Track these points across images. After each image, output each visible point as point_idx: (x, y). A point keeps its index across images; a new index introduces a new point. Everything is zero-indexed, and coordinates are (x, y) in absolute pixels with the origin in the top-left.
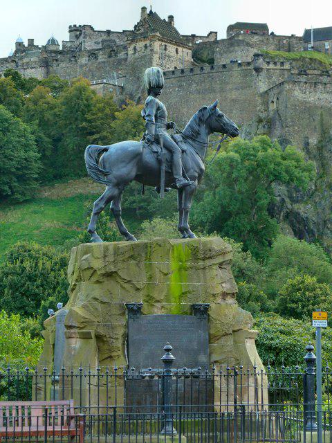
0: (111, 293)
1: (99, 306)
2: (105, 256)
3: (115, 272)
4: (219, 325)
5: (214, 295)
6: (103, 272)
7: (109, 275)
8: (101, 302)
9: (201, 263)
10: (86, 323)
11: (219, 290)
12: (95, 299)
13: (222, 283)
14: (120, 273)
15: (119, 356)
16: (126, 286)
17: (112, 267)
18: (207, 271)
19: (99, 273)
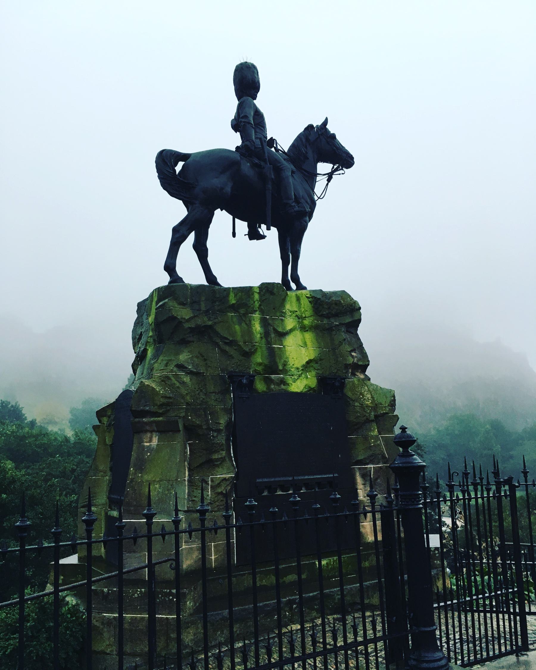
0: (205, 360)
1: (187, 379)
2: (193, 302)
3: (210, 327)
4: (358, 409)
5: (347, 366)
6: (192, 325)
7: (203, 332)
8: (190, 373)
9: (325, 321)
10: (169, 404)
11: (351, 360)
12: (180, 367)
13: (352, 351)
14: (218, 328)
15: (223, 460)
16: (227, 348)
17: (206, 319)
18: (334, 333)
19: (187, 325)
